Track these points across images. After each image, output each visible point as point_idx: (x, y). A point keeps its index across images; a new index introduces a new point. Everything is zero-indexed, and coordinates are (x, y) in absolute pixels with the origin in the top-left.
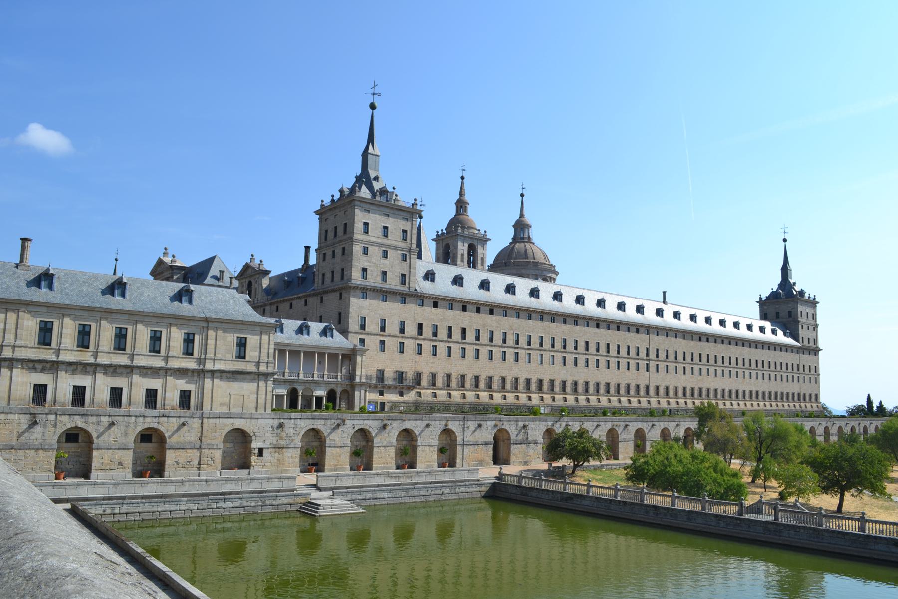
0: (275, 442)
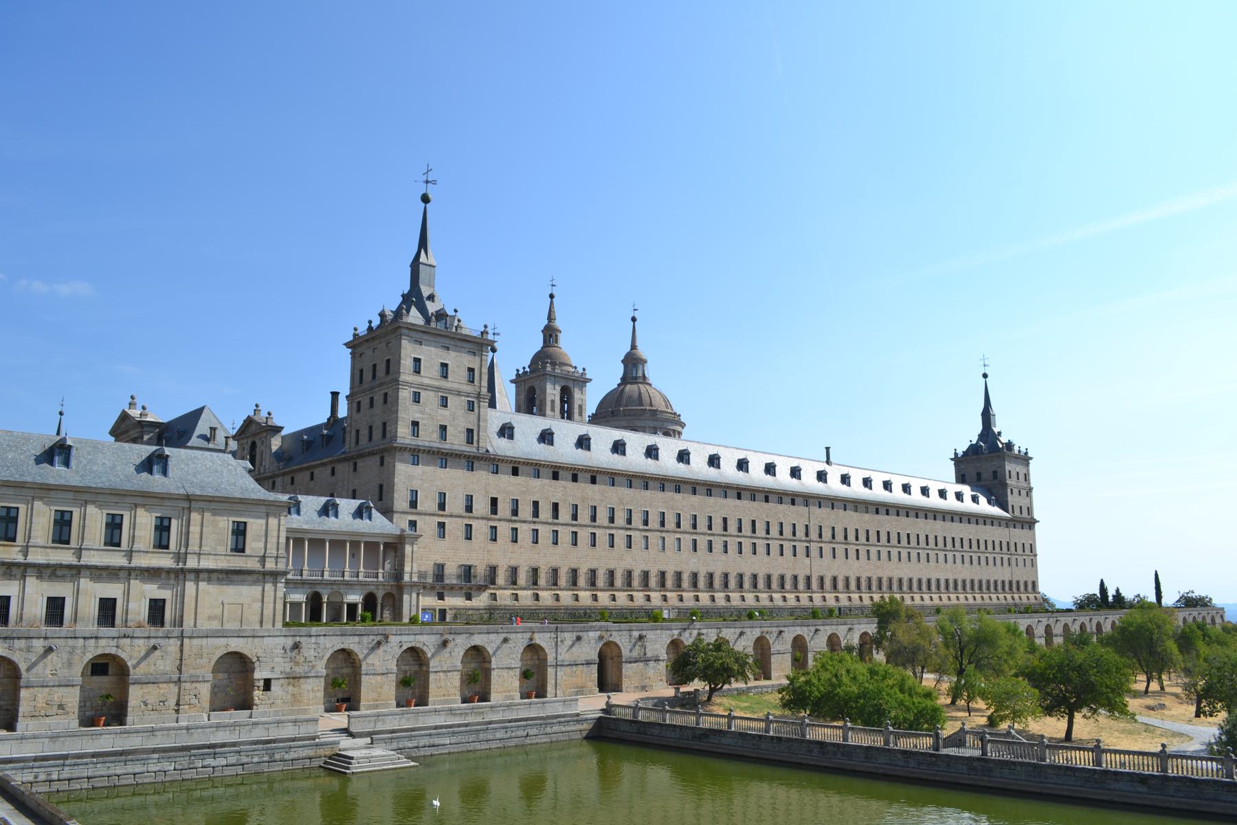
0: (288, 670)
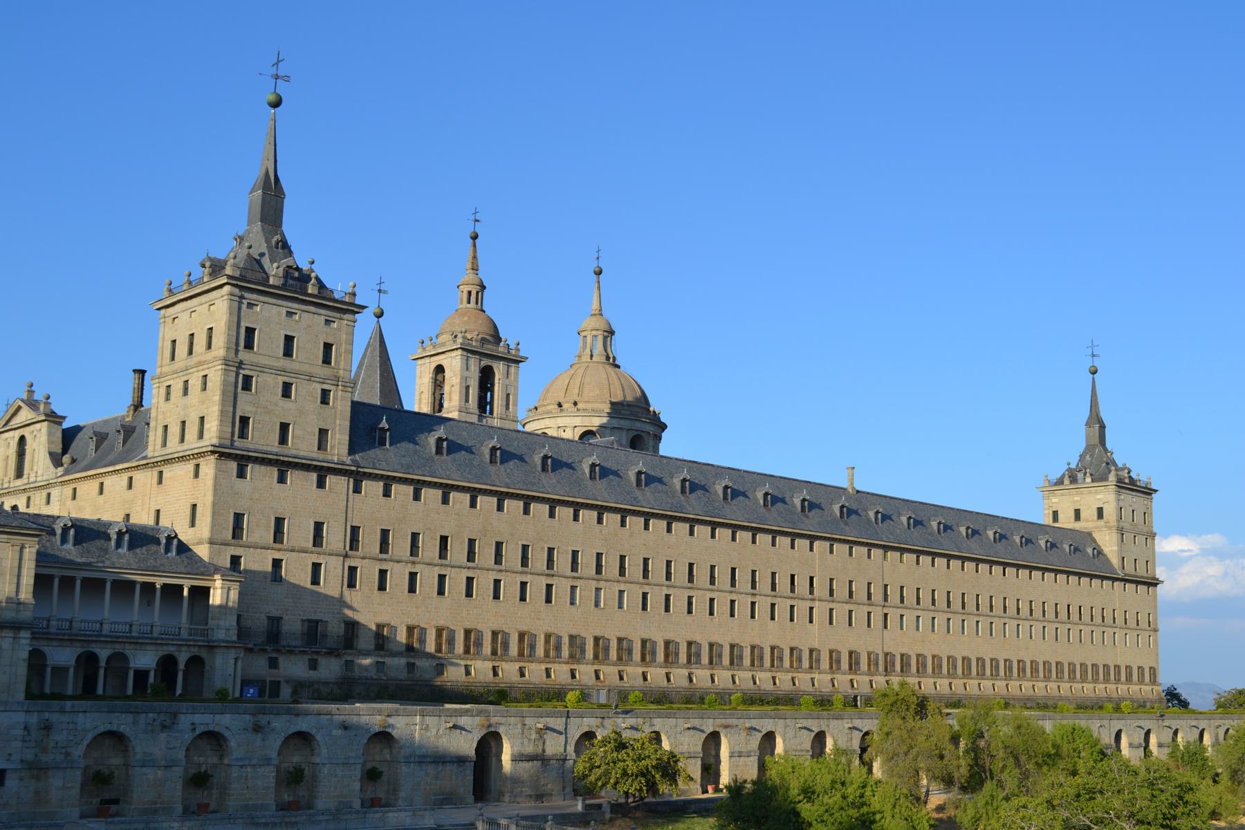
0: (29, 756)
